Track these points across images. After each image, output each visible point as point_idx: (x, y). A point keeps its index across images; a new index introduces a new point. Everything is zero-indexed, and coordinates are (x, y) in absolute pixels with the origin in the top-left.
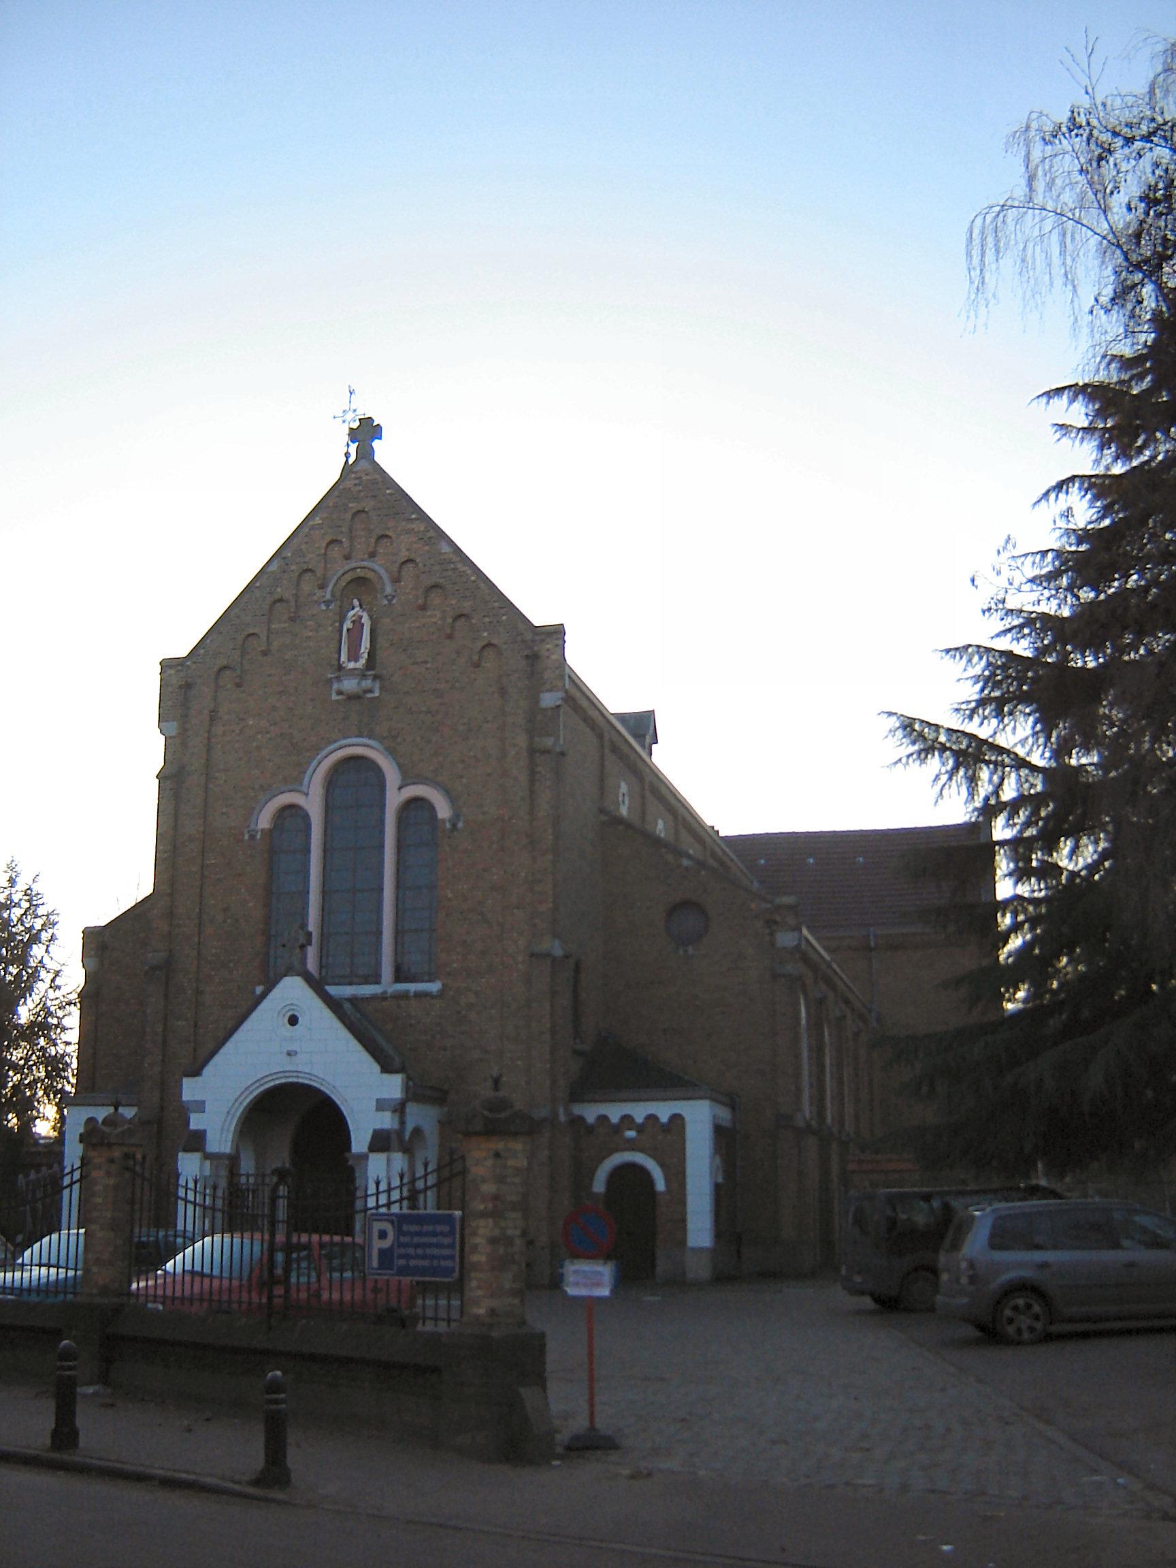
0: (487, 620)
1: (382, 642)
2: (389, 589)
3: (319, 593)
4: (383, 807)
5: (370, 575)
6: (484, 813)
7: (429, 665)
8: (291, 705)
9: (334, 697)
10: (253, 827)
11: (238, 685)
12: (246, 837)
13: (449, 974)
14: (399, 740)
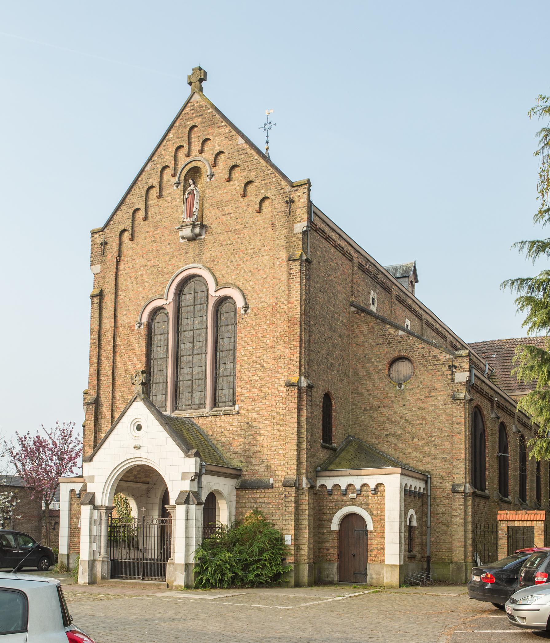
0: (263, 182)
1: (207, 204)
4: (207, 304)
7: (232, 215)
8: (158, 248)
9: (181, 241)
13: (243, 401)
14: (215, 263)
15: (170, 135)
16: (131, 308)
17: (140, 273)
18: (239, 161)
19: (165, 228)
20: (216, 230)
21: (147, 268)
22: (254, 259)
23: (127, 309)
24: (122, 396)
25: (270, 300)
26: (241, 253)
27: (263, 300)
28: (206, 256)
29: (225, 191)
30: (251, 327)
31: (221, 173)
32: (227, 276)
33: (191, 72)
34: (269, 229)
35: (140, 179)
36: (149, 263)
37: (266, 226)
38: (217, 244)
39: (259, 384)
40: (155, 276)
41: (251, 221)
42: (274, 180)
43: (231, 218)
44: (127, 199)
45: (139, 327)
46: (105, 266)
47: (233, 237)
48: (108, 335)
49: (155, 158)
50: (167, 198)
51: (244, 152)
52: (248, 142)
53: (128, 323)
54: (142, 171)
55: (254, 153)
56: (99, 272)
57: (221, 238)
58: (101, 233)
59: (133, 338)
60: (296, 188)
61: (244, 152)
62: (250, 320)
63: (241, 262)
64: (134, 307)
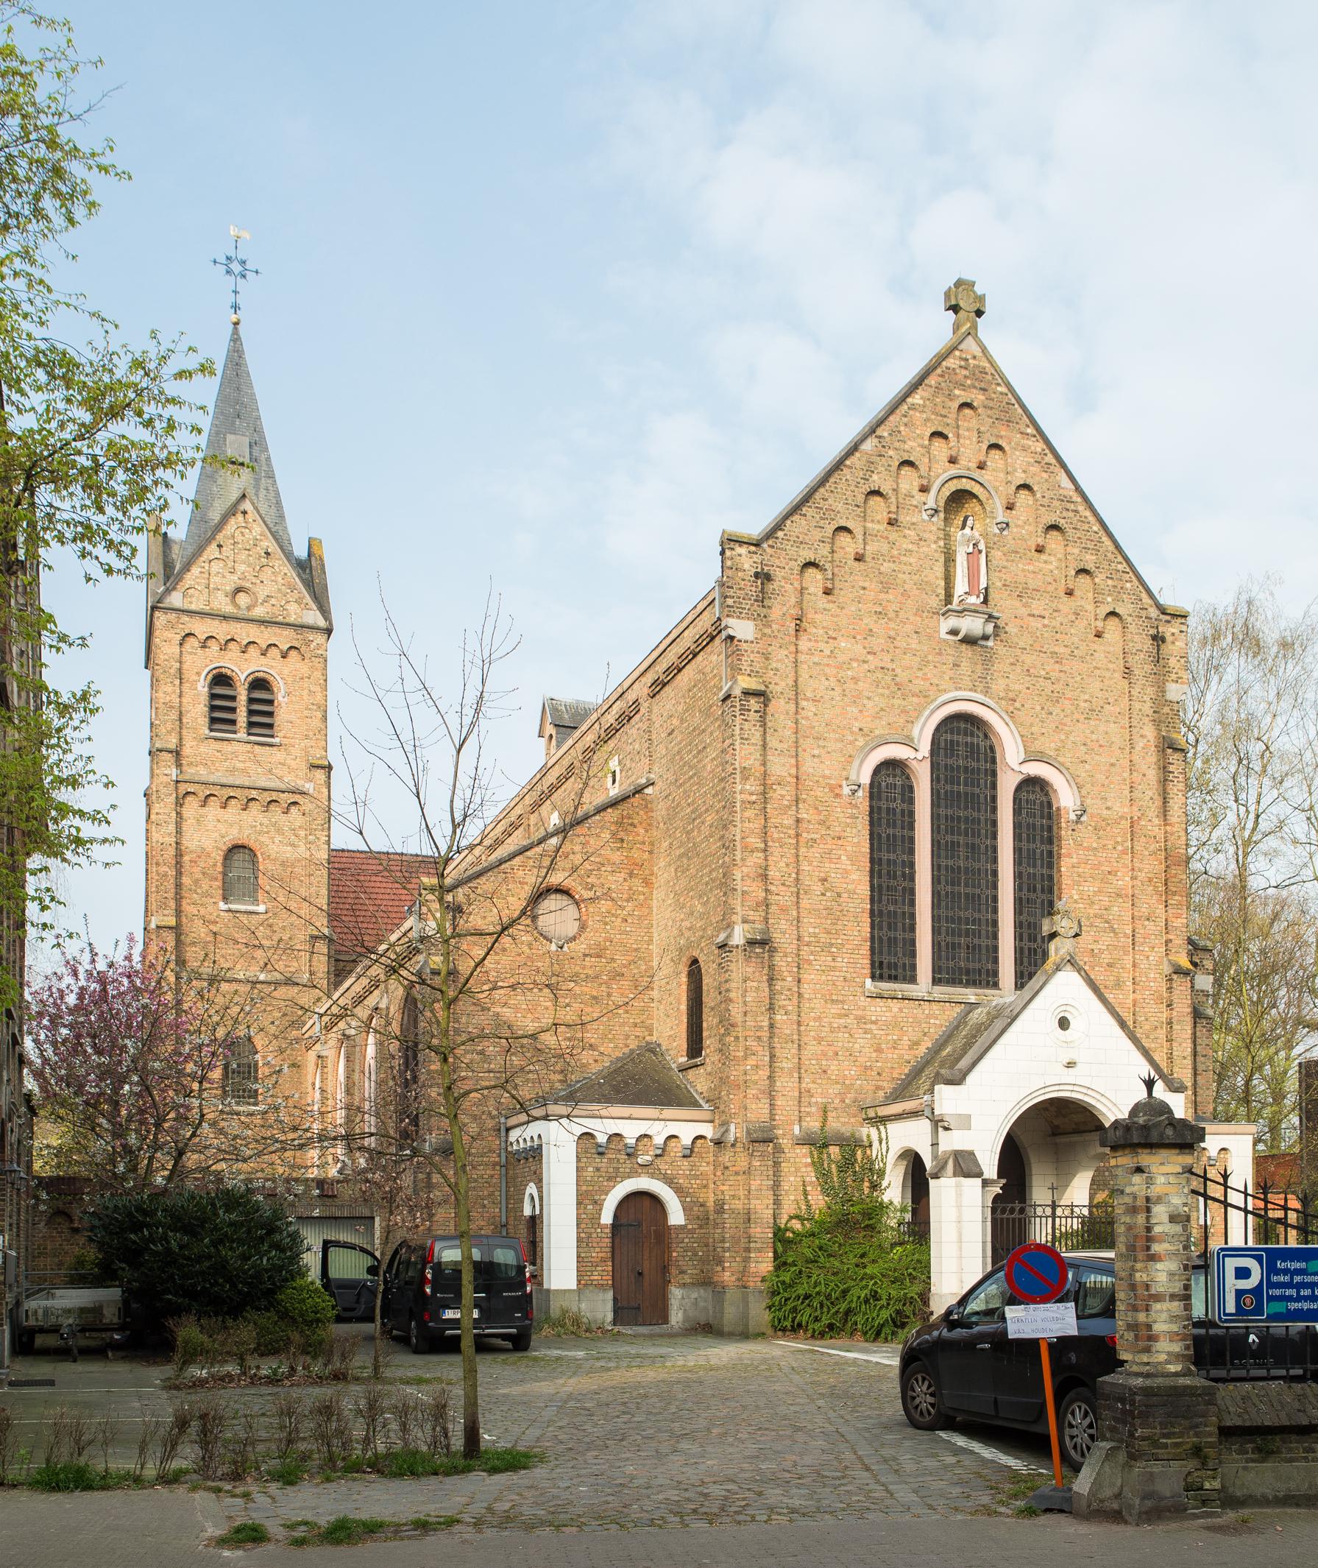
0: (1110, 582)
2: (1001, 515)
3: (920, 497)
5: (976, 489)
6: (1108, 808)
7: (1046, 621)
8: (892, 633)
10: (853, 777)
11: (827, 592)
14: (1017, 705)
15: (916, 399)
16: (832, 746)
17: (849, 673)
18: (1063, 521)
19: (905, 594)
20: (1016, 640)
21: (866, 666)
22: (1092, 723)
23: (821, 743)
24: (815, 935)
25: (1121, 808)
26: (1067, 702)
27: (1109, 804)
28: (999, 686)
29: (1031, 568)
30: (1088, 849)
31: (1022, 527)
32: (1042, 739)
33: (979, 290)
34: (1116, 675)
35: (848, 462)
36: (870, 657)
37: (1111, 666)
38: (1018, 669)
39: (1106, 958)
40: (887, 692)
41: (1083, 647)
42: (1128, 585)
43: (1045, 626)
44: (817, 496)
45: (854, 792)
46: (767, 631)
47: (1051, 666)
48: (780, 791)
50: (907, 532)
51: (1072, 507)
52: (1078, 489)
53: (824, 777)
54: (853, 449)
55: (1092, 519)
56: (750, 638)
57: (1028, 659)
58: (753, 548)
59: (840, 813)
60: (1168, 618)
61: (1072, 507)
62: (1085, 833)
63: (1067, 720)
64: (839, 745)
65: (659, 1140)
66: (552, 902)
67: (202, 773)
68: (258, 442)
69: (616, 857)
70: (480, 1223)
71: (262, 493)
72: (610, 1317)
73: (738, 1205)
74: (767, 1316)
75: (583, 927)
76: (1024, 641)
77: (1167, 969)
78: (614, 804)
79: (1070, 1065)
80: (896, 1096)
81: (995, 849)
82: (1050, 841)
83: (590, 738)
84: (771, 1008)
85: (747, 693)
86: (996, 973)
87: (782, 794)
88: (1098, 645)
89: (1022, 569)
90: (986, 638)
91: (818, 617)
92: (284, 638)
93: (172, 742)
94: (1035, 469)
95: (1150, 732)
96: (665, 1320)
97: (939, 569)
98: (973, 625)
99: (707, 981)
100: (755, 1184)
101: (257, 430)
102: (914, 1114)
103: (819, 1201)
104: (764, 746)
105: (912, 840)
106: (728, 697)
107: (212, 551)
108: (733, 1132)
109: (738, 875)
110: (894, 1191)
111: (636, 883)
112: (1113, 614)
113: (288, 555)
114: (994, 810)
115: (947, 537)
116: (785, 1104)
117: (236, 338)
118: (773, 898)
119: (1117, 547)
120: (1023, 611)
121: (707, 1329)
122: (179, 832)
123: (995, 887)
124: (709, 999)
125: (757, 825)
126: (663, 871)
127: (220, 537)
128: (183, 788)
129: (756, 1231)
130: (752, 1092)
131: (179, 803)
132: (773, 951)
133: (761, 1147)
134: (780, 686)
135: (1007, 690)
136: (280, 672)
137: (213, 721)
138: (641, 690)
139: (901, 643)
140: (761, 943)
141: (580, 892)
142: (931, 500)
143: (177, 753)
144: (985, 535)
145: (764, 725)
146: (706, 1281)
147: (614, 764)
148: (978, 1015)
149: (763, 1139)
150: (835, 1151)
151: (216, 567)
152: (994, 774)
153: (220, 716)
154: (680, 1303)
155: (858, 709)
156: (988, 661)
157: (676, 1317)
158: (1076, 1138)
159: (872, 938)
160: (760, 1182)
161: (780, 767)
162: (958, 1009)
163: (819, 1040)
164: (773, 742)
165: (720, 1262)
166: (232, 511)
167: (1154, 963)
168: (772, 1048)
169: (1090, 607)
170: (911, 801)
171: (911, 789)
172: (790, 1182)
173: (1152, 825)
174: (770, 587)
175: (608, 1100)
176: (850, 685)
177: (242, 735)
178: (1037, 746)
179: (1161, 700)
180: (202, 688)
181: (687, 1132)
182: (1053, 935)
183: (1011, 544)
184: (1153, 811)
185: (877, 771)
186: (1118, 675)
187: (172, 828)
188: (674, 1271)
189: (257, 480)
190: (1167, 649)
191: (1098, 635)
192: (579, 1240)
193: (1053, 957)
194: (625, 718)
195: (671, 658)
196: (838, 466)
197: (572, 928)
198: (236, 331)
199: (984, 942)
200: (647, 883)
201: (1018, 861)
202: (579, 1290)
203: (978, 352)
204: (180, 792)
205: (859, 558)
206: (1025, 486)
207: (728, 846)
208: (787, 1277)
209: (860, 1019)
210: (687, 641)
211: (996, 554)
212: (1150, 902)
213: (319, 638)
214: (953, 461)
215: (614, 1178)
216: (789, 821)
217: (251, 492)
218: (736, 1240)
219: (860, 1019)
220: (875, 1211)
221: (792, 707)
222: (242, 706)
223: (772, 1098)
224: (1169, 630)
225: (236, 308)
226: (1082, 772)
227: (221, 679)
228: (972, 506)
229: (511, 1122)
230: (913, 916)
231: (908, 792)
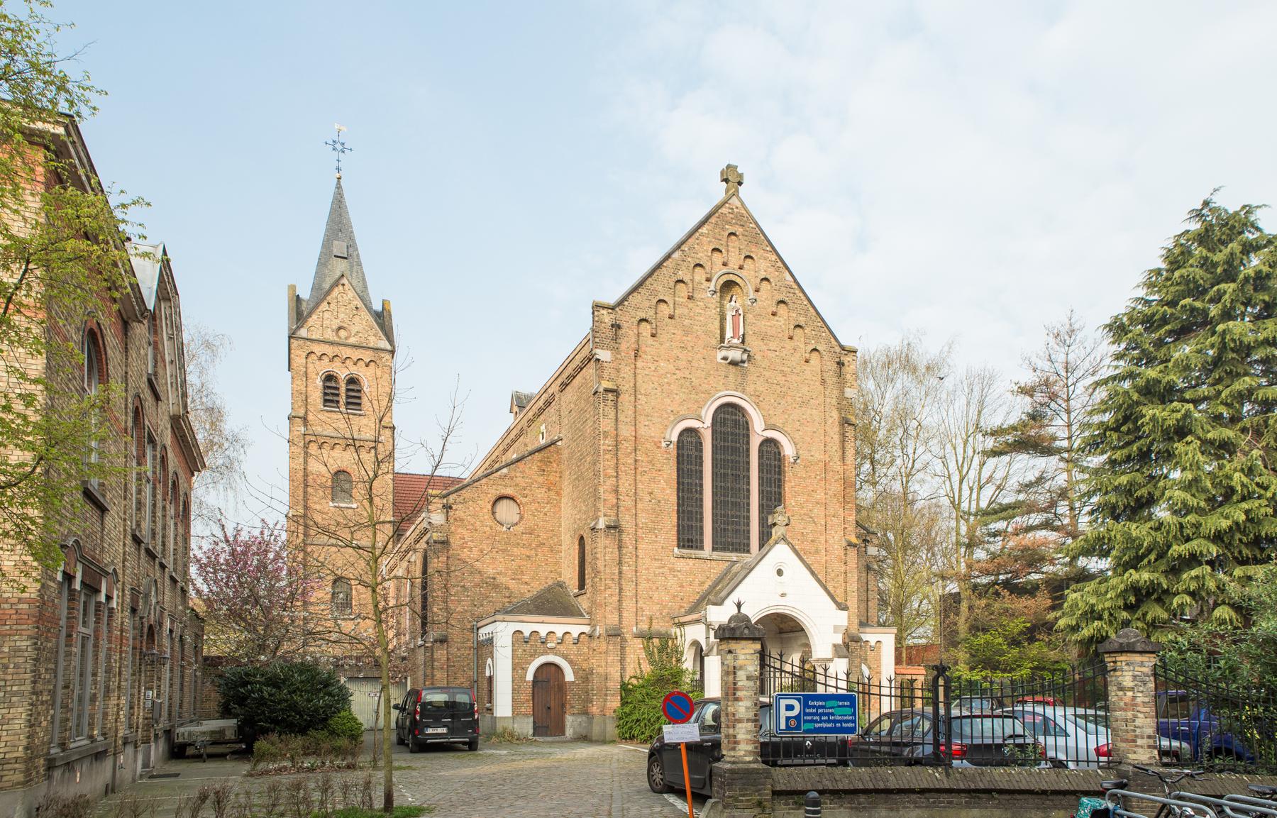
3: (706, 284)
5: (738, 280)
11: (653, 336)
12: (664, 445)
16: (655, 420)
25: (819, 456)
28: (750, 388)
39: (810, 537)
47: (781, 379)
48: (626, 444)
49: (685, 247)
52: (795, 281)
59: (659, 457)
62: (799, 470)
65: (559, 634)
66: (504, 505)
67: (319, 430)
68: (352, 245)
69: (541, 479)
70: (462, 680)
71: (355, 274)
72: (531, 732)
73: (601, 670)
74: (617, 731)
75: (522, 518)
76: (765, 364)
77: (844, 544)
78: (539, 450)
79: (783, 595)
80: (692, 610)
81: (748, 478)
82: (780, 473)
83: (531, 414)
84: (620, 563)
85: (606, 390)
86: (748, 545)
87: (627, 446)
88: (806, 366)
89: (765, 324)
90: (743, 362)
91: (648, 349)
92: (368, 355)
93: (301, 412)
94: (772, 270)
95: (835, 414)
96: (563, 734)
97: (717, 324)
98: (736, 355)
99: (587, 548)
100: (610, 659)
101: (351, 238)
102: (698, 621)
103: (647, 668)
104: (617, 420)
105: (701, 472)
106: (596, 393)
107: (324, 306)
108: (598, 630)
109: (601, 490)
110: (688, 663)
111: (552, 494)
112: (815, 350)
113: (369, 308)
114: (748, 456)
115: (722, 306)
116: (628, 616)
117: (339, 187)
118: (621, 503)
119: (818, 313)
120: (764, 348)
121: (584, 738)
122: (306, 462)
123: (748, 498)
124: (588, 558)
125: (613, 462)
126: (567, 488)
127: (329, 298)
128: (308, 438)
129: (610, 684)
130: (608, 609)
131: (306, 447)
132: (621, 532)
133: (614, 639)
134: (626, 387)
135: (755, 390)
136: (366, 376)
137: (326, 401)
138: (555, 388)
139: (695, 364)
140: (614, 528)
141: (520, 499)
142: (712, 286)
143: (305, 419)
144: (743, 306)
145: (616, 408)
146: (585, 712)
147: (543, 428)
148: (736, 568)
149: (615, 634)
150: (656, 641)
151: (326, 315)
152: (748, 436)
153: (330, 397)
154: (572, 724)
155: (673, 398)
156: (744, 374)
157: (569, 732)
158: (791, 635)
159: (678, 526)
160: (613, 658)
161: (626, 431)
162: (727, 564)
163: (648, 581)
164: (621, 417)
165: (591, 702)
166: (336, 284)
167: (837, 540)
168: (620, 584)
169: (802, 346)
170: (701, 451)
171: (701, 444)
172: (631, 658)
173: (837, 465)
174: (620, 332)
175: (530, 612)
176: (666, 387)
177: (343, 409)
178: (772, 421)
179: (841, 397)
180: (319, 383)
181: (575, 631)
182: (775, 524)
183: (758, 311)
184: (837, 457)
185: (681, 434)
186: (818, 383)
187: (301, 460)
188: (568, 706)
189: (352, 267)
190: (845, 369)
191: (807, 361)
192: (513, 689)
193: (774, 537)
194: (548, 403)
195: (569, 370)
196: (659, 266)
197: (516, 518)
198: (339, 183)
199: (742, 528)
200: (558, 494)
201: (761, 484)
202: (513, 718)
203: (739, 205)
204: (306, 441)
205: (671, 317)
206: (766, 279)
207: (596, 474)
208: (627, 710)
209: (671, 570)
210: (577, 362)
211: (749, 316)
212: (835, 507)
213: (388, 356)
214: (725, 264)
215: (534, 655)
216: (631, 461)
217: (347, 273)
218: (600, 690)
219: (671, 570)
220: (678, 674)
221: (632, 398)
222: (342, 393)
223: (620, 612)
224: (846, 359)
225: (339, 170)
226: (797, 436)
227: (330, 378)
228: (736, 290)
229: (480, 624)
230: (701, 513)
231: (699, 445)
